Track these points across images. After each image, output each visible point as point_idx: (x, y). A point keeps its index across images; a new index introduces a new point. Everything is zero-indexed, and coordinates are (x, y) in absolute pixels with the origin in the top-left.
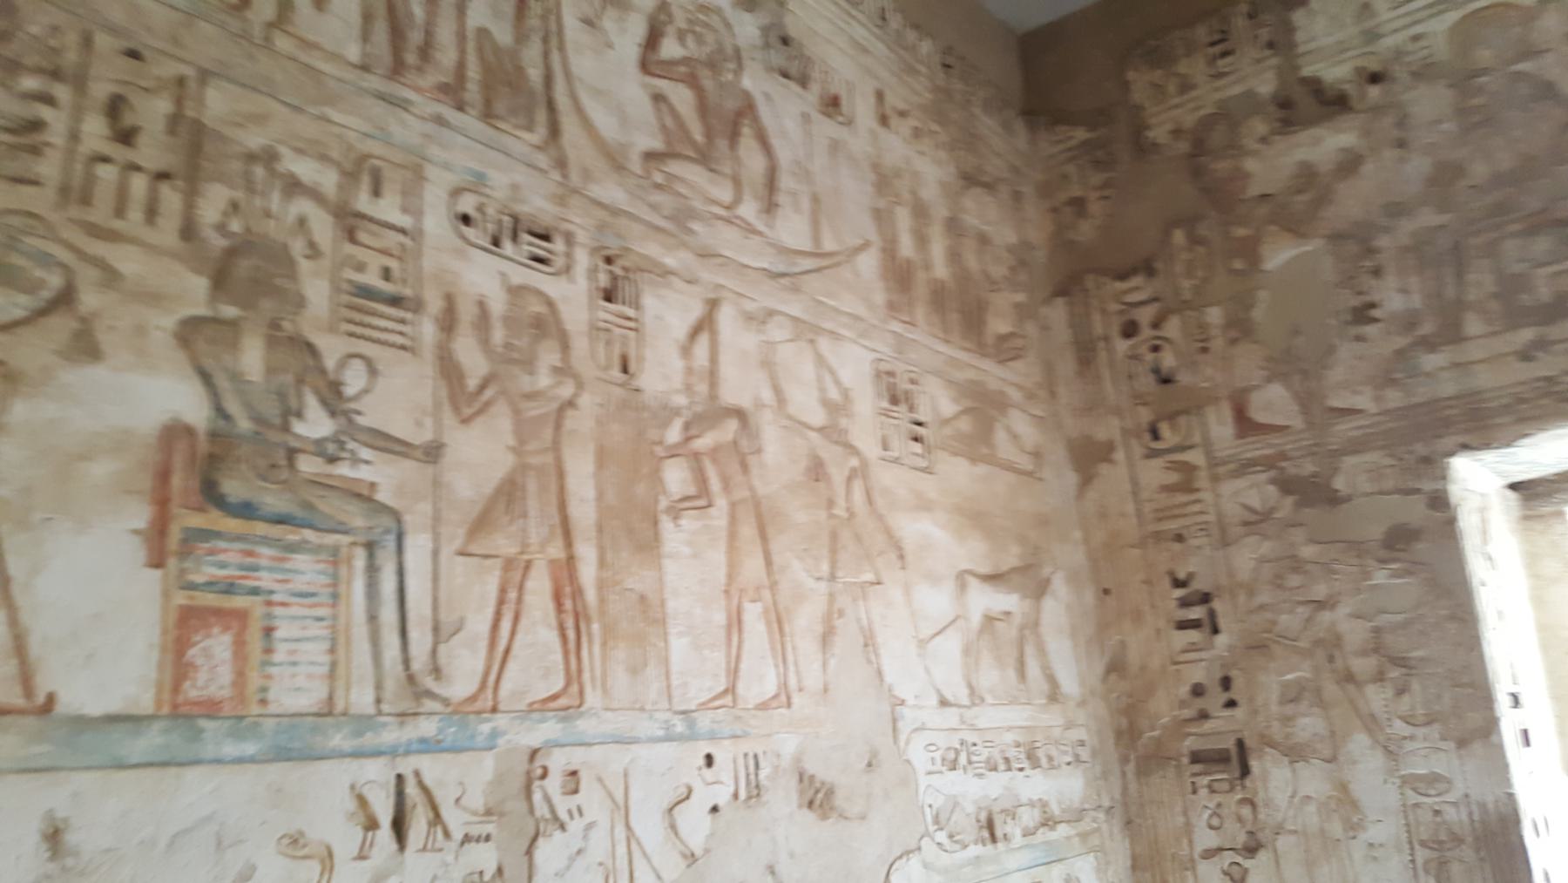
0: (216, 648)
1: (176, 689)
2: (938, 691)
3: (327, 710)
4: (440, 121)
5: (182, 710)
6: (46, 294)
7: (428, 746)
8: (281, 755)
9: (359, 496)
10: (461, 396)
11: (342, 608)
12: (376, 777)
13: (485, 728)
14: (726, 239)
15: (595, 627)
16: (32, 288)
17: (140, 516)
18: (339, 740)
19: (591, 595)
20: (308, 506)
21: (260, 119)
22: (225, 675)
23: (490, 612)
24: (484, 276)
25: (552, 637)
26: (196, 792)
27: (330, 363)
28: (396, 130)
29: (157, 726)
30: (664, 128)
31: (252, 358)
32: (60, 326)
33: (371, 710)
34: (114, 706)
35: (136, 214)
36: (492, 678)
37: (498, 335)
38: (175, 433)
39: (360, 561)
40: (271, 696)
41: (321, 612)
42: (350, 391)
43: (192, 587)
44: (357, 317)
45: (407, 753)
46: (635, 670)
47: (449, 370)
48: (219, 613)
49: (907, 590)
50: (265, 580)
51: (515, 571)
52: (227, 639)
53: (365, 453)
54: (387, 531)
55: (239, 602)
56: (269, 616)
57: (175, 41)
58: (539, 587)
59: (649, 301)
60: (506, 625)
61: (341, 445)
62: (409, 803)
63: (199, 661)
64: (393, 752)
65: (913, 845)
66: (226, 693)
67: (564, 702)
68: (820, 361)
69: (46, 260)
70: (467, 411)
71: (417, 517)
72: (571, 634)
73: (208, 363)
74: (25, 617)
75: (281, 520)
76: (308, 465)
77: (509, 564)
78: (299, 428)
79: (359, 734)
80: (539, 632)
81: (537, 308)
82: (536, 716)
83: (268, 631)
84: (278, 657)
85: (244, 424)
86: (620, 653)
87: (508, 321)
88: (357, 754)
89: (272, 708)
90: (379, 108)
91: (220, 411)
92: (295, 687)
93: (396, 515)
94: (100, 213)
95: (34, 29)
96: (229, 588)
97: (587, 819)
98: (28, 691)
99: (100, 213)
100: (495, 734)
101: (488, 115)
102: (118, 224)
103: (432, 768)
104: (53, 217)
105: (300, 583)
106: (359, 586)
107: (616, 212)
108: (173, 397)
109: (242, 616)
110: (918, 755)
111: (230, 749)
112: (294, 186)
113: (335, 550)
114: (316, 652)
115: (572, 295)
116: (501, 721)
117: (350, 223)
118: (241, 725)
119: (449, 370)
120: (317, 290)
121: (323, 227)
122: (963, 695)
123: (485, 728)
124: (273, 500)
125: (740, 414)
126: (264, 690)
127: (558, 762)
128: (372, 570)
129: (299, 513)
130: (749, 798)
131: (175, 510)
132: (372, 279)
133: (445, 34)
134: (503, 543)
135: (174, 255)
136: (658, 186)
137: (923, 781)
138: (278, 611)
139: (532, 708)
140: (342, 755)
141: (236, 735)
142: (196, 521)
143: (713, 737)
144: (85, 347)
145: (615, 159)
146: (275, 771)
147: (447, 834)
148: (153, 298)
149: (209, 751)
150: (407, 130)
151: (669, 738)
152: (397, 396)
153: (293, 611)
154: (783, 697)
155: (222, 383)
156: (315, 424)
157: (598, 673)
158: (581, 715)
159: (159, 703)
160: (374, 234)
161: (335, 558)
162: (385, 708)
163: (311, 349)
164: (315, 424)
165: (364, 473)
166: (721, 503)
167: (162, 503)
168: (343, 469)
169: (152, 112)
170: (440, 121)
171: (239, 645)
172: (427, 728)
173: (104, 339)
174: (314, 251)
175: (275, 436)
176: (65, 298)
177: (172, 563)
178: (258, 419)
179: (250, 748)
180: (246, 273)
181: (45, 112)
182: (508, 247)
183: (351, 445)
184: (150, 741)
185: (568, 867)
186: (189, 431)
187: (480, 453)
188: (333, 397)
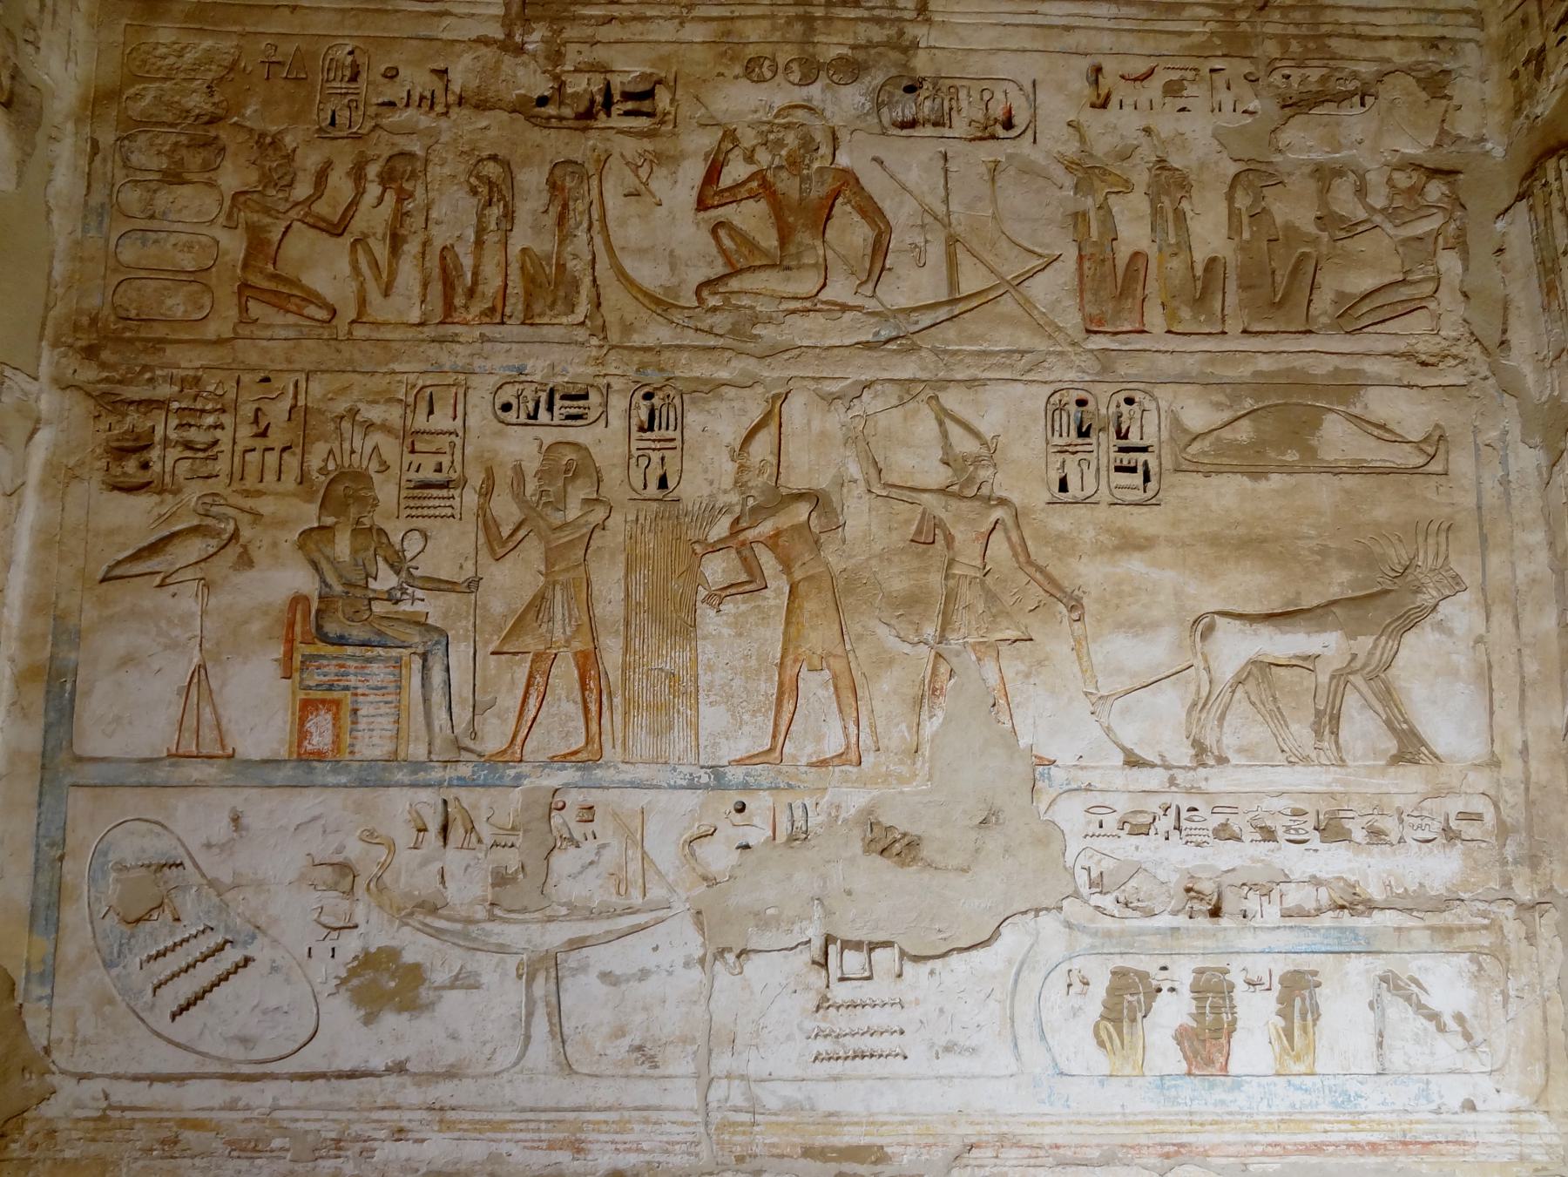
1: (299, 746)
2: (1124, 749)
3: (393, 758)
4: (484, 339)
5: (306, 759)
6: (226, 536)
7: (464, 783)
8: (363, 783)
9: (417, 623)
10: (497, 543)
11: (404, 695)
12: (427, 800)
13: (512, 772)
14: (802, 331)
15: (617, 700)
16: (219, 534)
17: (279, 651)
18: (400, 776)
19: (615, 676)
20: (380, 633)
21: (344, 390)
22: (328, 738)
23: (520, 693)
24: (521, 447)
25: (575, 710)
26: (307, 803)
27: (396, 539)
28: (447, 362)
29: (289, 765)
30: (723, 251)
31: (343, 546)
32: (233, 552)
33: (424, 758)
34: (266, 755)
35: (270, 477)
36: (519, 740)
37: (531, 486)
38: (298, 600)
39: (417, 663)
40: (356, 749)
41: (389, 698)
42: (409, 555)
43: (309, 688)
44: (418, 503)
45: (450, 786)
46: (656, 733)
47: (488, 524)
48: (323, 702)
49: (1079, 646)
50: (353, 681)
51: (542, 664)
52: (329, 717)
53: (419, 594)
54: (437, 643)
55: (335, 695)
57: (289, 361)
58: (565, 674)
59: (693, 418)
60: (533, 702)
61: (404, 592)
62: (451, 818)
63: (313, 730)
64: (440, 785)
65: (1050, 903)
66: (330, 747)
67: (586, 758)
68: (944, 416)
69: (227, 518)
70: (500, 552)
71: (458, 630)
72: (593, 708)
73: (316, 556)
74: (221, 711)
75: (364, 644)
76: (378, 608)
77: (538, 656)
78: (373, 584)
79: (415, 772)
80: (563, 703)
81: (569, 455)
82: (556, 765)
83: (355, 711)
84: (360, 727)
85: (338, 589)
86: (641, 720)
87: (540, 474)
88: (413, 785)
89: (358, 756)
90: (433, 350)
91: (324, 581)
92: (373, 742)
93: (442, 633)
94: (251, 482)
95: (211, 388)
96: (331, 688)
97: (600, 841)
98: (223, 747)
99: (251, 482)
100: (519, 777)
101: (528, 320)
102: (260, 486)
103: (467, 797)
104: (226, 492)
105: (373, 682)
106: (416, 680)
107: (657, 350)
108: (298, 579)
109: (337, 703)
110: (1070, 815)
111: (331, 779)
112: (369, 426)
113: (399, 660)
114: (386, 722)
115: (607, 438)
116: (524, 768)
117: (411, 439)
118: (338, 766)
119: (488, 524)
120: (386, 492)
121: (390, 448)
122: (1182, 754)
123: (512, 772)
124: (358, 633)
125: (816, 498)
126: (352, 745)
127: (574, 798)
128: (425, 668)
129: (375, 639)
130: (792, 838)
131: (297, 644)
132: (428, 474)
133: (490, 270)
134: (531, 643)
135: (294, 495)
136: (715, 309)
137: (1073, 848)
138: (361, 699)
139: (552, 759)
140: (403, 785)
141: (334, 771)
142: (308, 650)
143: (746, 787)
144: (246, 561)
145: (661, 305)
146: (357, 793)
147: (480, 841)
148: (282, 524)
149: (319, 780)
150: (459, 355)
151: (692, 786)
152: (446, 548)
154: (850, 757)
155: (324, 565)
156: (386, 580)
157: (619, 735)
158: (599, 766)
159: (291, 753)
160: (427, 442)
162: (434, 757)
163: (381, 531)
164: (386, 580)
165: (419, 607)
166: (778, 586)
167: (290, 641)
168: (405, 607)
169: (278, 411)
170: (484, 339)
171: (336, 718)
172: (465, 770)
173: (255, 554)
174: (385, 467)
175: (359, 592)
176: (235, 536)
177: (296, 676)
178: (349, 584)
179: (343, 779)
180: (344, 493)
181: (218, 433)
182: (543, 416)
183: (410, 590)
184: (285, 773)
185: (581, 873)
186: (306, 599)
187: (513, 580)
188: (397, 563)
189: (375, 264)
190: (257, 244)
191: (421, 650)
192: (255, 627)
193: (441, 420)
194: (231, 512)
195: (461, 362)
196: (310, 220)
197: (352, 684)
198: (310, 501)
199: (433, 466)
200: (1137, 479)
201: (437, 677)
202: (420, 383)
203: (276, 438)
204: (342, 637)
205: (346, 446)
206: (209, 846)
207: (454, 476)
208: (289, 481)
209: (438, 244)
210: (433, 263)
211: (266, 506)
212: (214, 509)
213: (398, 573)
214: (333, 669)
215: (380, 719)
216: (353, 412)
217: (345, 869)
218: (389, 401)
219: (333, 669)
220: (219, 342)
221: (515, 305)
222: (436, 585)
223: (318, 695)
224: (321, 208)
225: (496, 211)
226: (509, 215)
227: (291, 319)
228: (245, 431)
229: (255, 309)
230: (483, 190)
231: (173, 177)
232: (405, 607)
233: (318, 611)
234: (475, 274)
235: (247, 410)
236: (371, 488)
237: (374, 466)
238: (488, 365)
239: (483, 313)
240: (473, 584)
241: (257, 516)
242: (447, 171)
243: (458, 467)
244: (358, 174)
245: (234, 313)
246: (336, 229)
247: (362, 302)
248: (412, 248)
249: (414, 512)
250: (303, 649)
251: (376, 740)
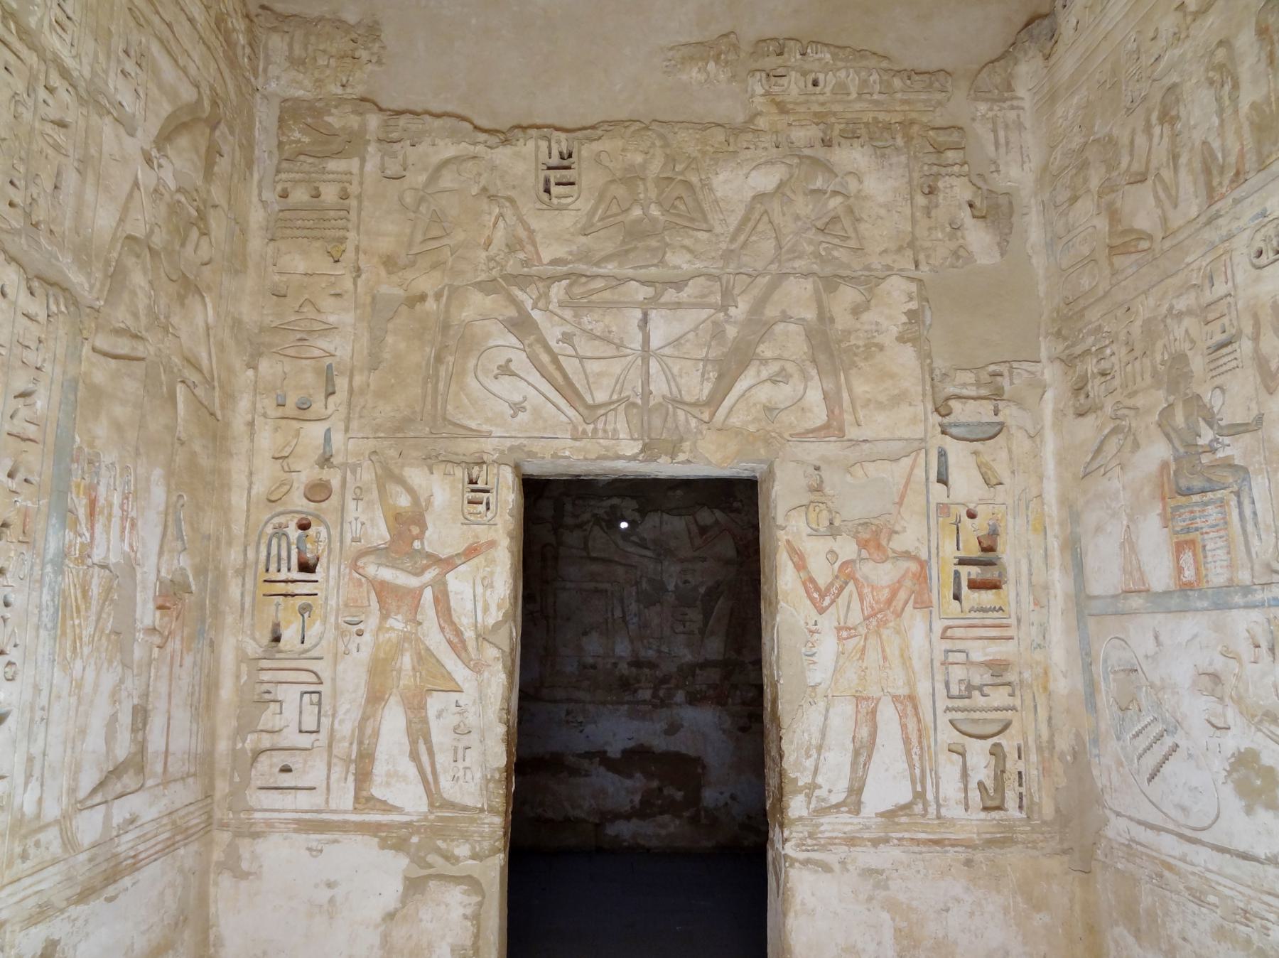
0: (1187, 558)
17: (1158, 508)
20: (1209, 480)
22: (1193, 572)
39: (1234, 503)
42: (1216, 410)
45: (1270, 606)
53: (1227, 440)
56: (1203, 540)
73: (1168, 429)
79: (1245, 595)
83: (1204, 547)
89: (1211, 585)
102: (1135, 388)
105: (1211, 521)
109: (1193, 542)
111: (1199, 604)
113: (1222, 500)
114: (1221, 553)
117: (1204, 313)
120: (1197, 363)
124: (1197, 483)
128: (1240, 504)
129: (1207, 485)
132: (1219, 337)
140: (1240, 607)
141: (1200, 598)
153: (1211, 535)
155: (1173, 435)
156: (1207, 436)
161: (1222, 503)
167: (1163, 499)
168: (1220, 454)
170: (1236, 202)
171: (1195, 555)
178: (1188, 445)
179: (1205, 604)
180: (1176, 374)
184: (1175, 602)
191: (1235, 488)
192: (1146, 491)
193: (1221, 288)
194: (1126, 412)
195: (1224, 232)
196: (1132, 180)
197: (1199, 525)
198: (1159, 389)
199: (1219, 330)
202: (1204, 264)
204: (1188, 489)
205: (1172, 337)
206: (1147, 657)
207: (1234, 331)
208: (1148, 379)
209: (1198, 143)
210: (1197, 165)
211: (1139, 401)
212: (1119, 412)
213: (1211, 427)
214: (1187, 516)
215: (1219, 552)
216: (1171, 308)
217: (1215, 678)
218: (1188, 289)
219: (1187, 516)
220: (1106, 294)
221: (1250, 162)
222: (1237, 430)
223: (1183, 537)
224: (1136, 167)
225: (1227, 88)
226: (1236, 86)
228: (1124, 350)
230: (1217, 77)
232: (1220, 454)
233: (1175, 472)
234: (1223, 150)
235: (1122, 337)
236: (1188, 365)
237: (1187, 345)
238: (1241, 223)
239: (1232, 181)
240: (1260, 419)
241: (1136, 409)
242: (1194, 81)
243: (1235, 323)
244: (1148, 128)
246: (1141, 179)
248: (1183, 160)
249: (1214, 373)
250: (1172, 503)
251: (1219, 570)
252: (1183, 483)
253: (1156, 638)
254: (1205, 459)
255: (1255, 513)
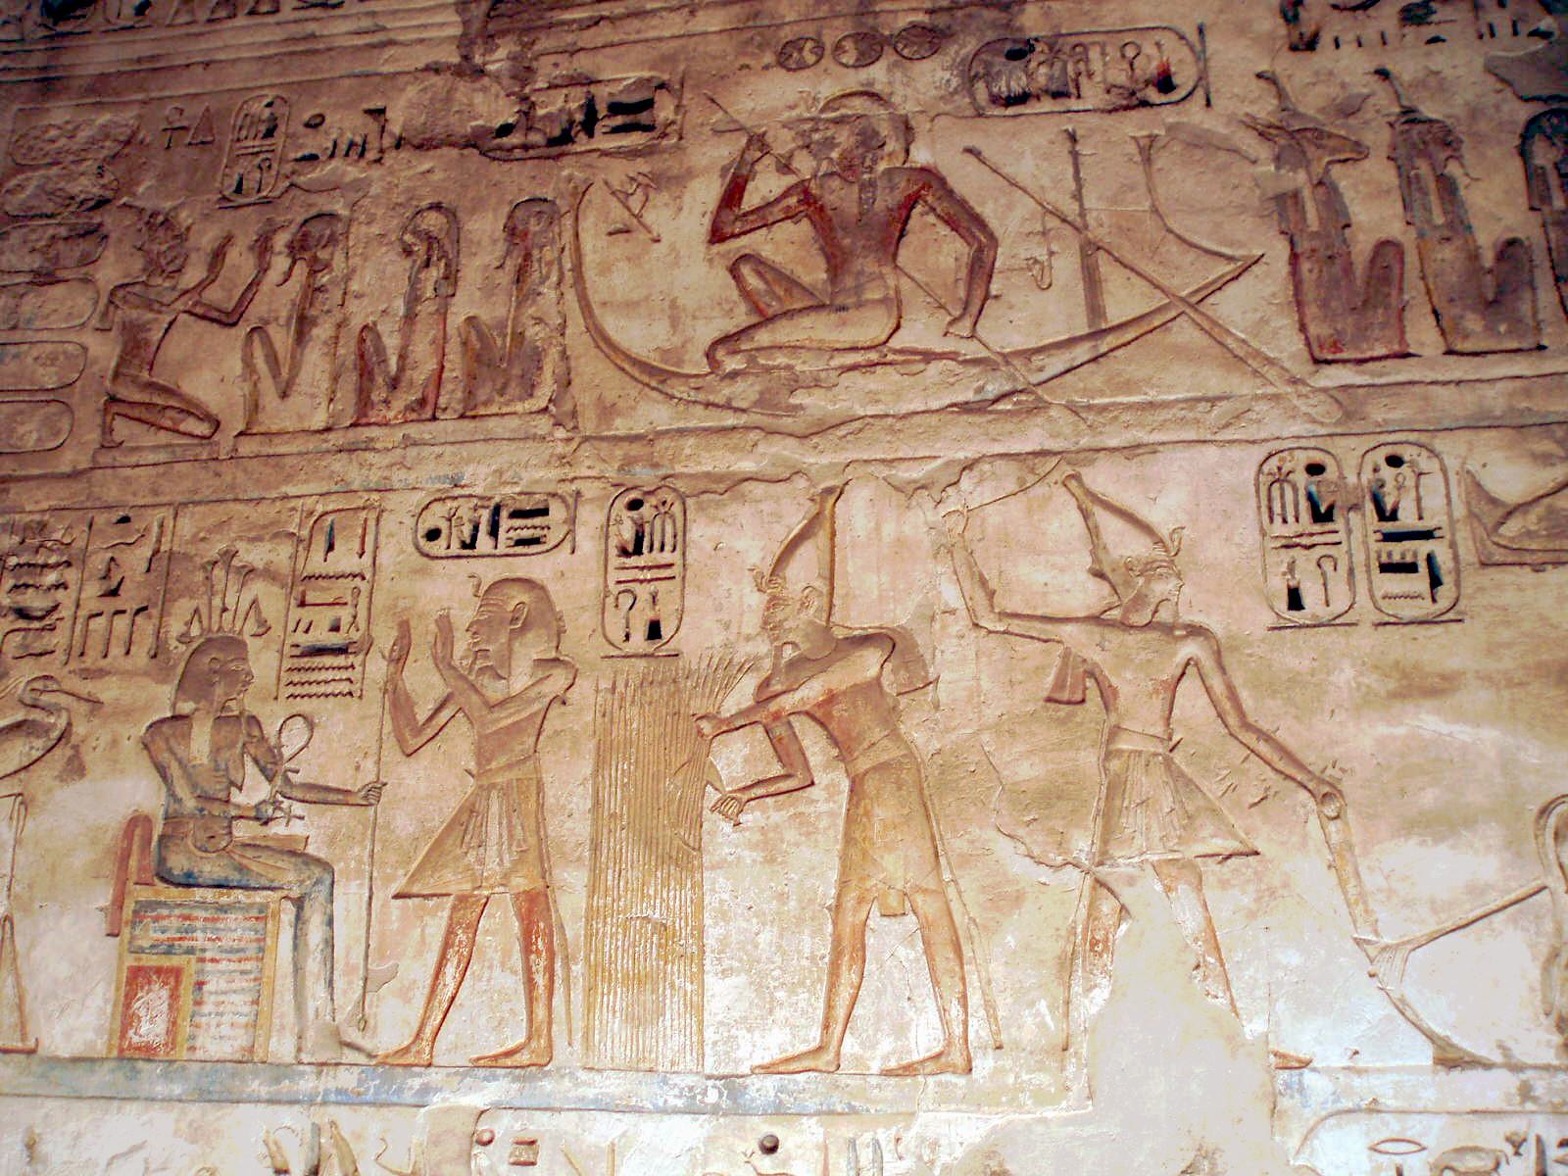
0: (154, 1001)
2: (1431, 1037)
3: (246, 1059)
5: (131, 1055)
6: (55, 734)
7: (350, 1099)
8: (204, 1096)
9: (293, 853)
10: (411, 730)
13: (416, 1083)
15: (577, 969)
17: (104, 897)
19: (574, 930)
20: (241, 869)
21: (221, 526)
22: (161, 1026)
23: (432, 958)
24: (450, 590)
25: (514, 983)
27: (270, 730)
28: (356, 477)
30: (746, 294)
31: (200, 743)
32: (62, 753)
33: (289, 1058)
35: (116, 651)
37: (461, 645)
38: (138, 822)
39: (288, 912)
40: (198, 1043)
41: (248, 966)
42: (287, 752)
43: (142, 950)
45: (324, 1103)
46: (636, 1020)
48: (159, 971)
49: (1341, 860)
50: (200, 939)
51: (467, 911)
52: (165, 993)
53: (298, 808)
55: (175, 961)
56: (201, 972)
57: (155, 493)
58: (500, 927)
59: (700, 532)
60: (450, 971)
61: (277, 806)
63: (142, 1013)
66: (162, 1039)
70: (414, 743)
71: (349, 860)
72: (541, 980)
73: (165, 757)
74: (25, 982)
77: (462, 899)
78: (237, 797)
79: (278, 1080)
82: (481, 1072)
83: (200, 985)
84: (206, 1009)
89: (199, 1054)
90: (338, 464)
91: (172, 794)
92: (219, 1034)
93: (326, 866)
95: (58, 536)
96: (169, 952)
98: (24, 1037)
102: (103, 663)
103: (347, 1119)
108: (138, 791)
109: (177, 973)
111: (160, 1089)
112: (249, 572)
113: (263, 908)
114: (240, 1003)
115: (573, 570)
116: (434, 1076)
117: (301, 588)
120: (263, 662)
121: (272, 600)
123: (416, 1083)
124: (211, 868)
125: (888, 641)
126: (193, 1037)
129: (235, 877)
131: (130, 885)
132: (322, 636)
134: (454, 882)
135: (146, 674)
136: (734, 375)
138: (209, 966)
139: (477, 1063)
141: (166, 1076)
142: (144, 894)
143: (778, 1111)
144: (76, 768)
145: (655, 375)
146: (194, 1111)
148: (127, 713)
151: (692, 1110)
153: (223, 966)
154: (950, 1060)
155: (175, 770)
156: (255, 790)
157: (579, 1024)
158: (547, 1074)
159: (110, 1050)
160: (323, 589)
161: (262, 915)
163: (254, 720)
164: (255, 790)
165: (297, 828)
168: (278, 829)
170: (408, 442)
171: (174, 996)
172: (347, 1079)
173: (89, 757)
174: (264, 628)
177: (126, 932)
178: (204, 797)
179: (177, 1089)
180: (210, 667)
181: (60, 594)
182: (484, 543)
183: (286, 804)
184: (102, 1078)
188: (271, 765)
189: (273, 360)
190: (136, 347)
191: (295, 893)
193: (345, 559)
194: (63, 700)
195: (374, 477)
196: (199, 310)
197: (198, 944)
198: (164, 681)
199: (327, 625)
200: (1419, 582)
201: (315, 933)
202: (320, 509)
203: (129, 600)
204: (189, 875)
205: (217, 602)
207: (355, 636)
208: (141, 656)
209: (356, 323)
210: (347, 350)
211: (108, 691)
212: (45, 698)
213: (270, 779)
215: (234, 998)
216: (230, 555)
218: (276, 535)
219: (175, 923)
220: (75, 475)
221: (451, 395)
222: (323, 795)
223: (151, 961)
224: (214, 295)
225: (435, 273)
226: (451, 277)
227: (163, 437)
228: (93, 589)
229: (122, 429)
230: (420, 248)
231: (44, 278)
232: (278, 829)
233: (162, 837)
234: (402, 357)
235: (98, 562)
236: (245, 660)
237: (251, 627)
238: (412, 477)
239: (409, 408)
240: (374, 792)
241: (95, 703)
242: (375, 230)
243: (362, 622)
244: (263, 247)
245: (94, 436)
246: (227, 319)
247: (254, 407)
248: (322, 332)
249: (298, 690)
251: (225, 1030)
252: (178, 863)
253: (31, 1146)
254: (243, 831)
255: (329, 943)
